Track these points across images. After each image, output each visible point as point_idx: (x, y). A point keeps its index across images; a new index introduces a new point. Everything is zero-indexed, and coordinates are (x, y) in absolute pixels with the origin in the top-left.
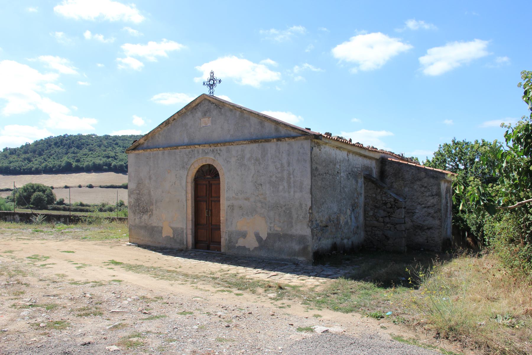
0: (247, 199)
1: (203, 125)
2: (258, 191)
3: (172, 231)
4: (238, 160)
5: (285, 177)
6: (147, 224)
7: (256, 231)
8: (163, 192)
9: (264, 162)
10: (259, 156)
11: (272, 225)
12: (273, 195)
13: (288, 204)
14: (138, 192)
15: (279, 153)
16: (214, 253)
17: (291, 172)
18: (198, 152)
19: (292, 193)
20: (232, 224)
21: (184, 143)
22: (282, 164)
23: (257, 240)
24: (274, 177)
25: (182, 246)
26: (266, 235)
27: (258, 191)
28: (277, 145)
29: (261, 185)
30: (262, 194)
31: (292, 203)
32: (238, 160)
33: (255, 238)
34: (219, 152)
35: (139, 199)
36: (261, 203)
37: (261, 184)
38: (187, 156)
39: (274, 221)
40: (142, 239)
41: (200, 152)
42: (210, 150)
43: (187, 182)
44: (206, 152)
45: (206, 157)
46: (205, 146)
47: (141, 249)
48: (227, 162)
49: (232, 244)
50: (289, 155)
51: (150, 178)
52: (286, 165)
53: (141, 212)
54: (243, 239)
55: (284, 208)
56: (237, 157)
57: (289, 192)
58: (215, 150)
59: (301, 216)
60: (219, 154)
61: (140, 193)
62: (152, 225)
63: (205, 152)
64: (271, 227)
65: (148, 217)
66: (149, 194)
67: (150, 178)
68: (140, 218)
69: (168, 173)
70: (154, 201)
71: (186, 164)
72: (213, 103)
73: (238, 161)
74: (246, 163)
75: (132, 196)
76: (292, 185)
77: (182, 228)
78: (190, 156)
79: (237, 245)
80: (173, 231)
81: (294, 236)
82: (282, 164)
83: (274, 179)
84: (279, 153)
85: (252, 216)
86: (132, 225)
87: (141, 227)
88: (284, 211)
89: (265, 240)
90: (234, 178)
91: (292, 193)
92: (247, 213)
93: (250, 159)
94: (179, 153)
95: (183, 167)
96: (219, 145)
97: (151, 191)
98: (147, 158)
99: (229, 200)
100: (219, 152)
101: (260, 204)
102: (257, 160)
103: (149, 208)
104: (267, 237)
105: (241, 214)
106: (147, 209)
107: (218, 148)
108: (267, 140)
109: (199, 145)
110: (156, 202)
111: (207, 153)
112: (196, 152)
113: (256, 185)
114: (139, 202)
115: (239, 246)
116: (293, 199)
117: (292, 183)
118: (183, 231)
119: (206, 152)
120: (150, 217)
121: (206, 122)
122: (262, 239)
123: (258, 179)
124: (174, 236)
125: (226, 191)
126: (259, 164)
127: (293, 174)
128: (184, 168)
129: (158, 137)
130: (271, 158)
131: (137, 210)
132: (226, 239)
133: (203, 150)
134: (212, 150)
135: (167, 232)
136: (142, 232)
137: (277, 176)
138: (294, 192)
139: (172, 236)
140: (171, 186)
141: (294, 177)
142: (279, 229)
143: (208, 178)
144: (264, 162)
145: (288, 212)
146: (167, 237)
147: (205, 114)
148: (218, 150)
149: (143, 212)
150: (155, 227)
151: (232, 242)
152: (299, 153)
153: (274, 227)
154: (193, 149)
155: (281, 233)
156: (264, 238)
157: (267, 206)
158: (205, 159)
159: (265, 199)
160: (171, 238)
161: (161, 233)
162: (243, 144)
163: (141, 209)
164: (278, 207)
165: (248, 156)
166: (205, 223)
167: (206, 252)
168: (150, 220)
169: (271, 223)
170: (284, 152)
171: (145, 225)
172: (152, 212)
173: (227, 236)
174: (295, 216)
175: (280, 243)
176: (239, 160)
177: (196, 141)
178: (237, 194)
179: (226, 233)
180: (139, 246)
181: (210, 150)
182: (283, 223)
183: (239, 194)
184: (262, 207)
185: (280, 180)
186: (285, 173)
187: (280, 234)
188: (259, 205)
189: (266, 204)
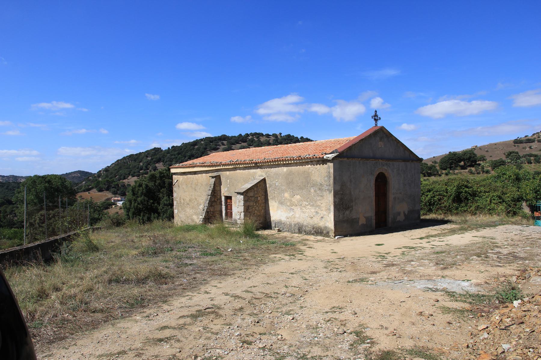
0: (401, 193)
1: (380, 146)
14: (342, 192)
51: (351, 181)
68: (344, 214)
77: (371, 216)
79: (397, 220)
108: (408, 161)
120: (351, 212)
121: (381, 144)
135: (362, 221)
139: (365, 223)
142: (411, 208)
147: (381, 139)
149: (346, 209)
150: (355, 218)
156: (406, 214)
161: (358, 222)
172: (352, 208)
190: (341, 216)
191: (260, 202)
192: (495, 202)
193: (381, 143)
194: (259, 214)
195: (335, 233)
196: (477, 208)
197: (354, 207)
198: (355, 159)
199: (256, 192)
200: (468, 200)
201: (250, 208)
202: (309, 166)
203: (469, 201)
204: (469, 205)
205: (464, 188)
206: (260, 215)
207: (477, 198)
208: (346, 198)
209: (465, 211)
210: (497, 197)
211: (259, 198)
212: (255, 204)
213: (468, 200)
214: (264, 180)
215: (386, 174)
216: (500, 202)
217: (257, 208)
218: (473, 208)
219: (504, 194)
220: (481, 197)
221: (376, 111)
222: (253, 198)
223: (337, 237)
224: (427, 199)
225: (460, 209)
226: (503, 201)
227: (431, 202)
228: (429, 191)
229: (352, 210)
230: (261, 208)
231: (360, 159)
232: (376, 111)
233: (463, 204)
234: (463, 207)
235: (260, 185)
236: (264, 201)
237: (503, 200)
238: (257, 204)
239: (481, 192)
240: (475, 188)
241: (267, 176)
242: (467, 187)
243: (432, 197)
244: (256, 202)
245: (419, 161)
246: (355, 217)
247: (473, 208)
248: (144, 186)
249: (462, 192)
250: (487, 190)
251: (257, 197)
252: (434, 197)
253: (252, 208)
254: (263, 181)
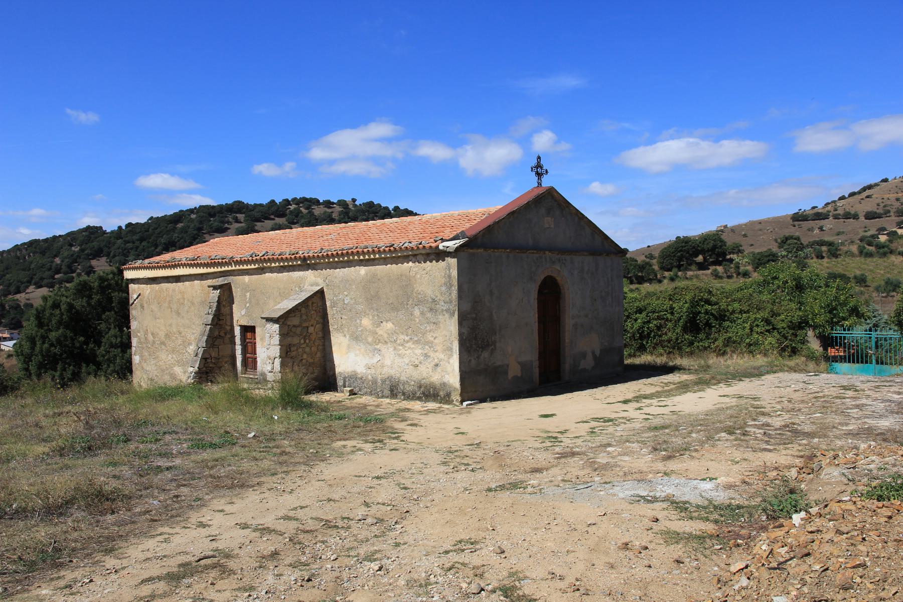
0: (586, 316)
1: (547, 226)
29: (595, 300)
60: (564, 264)
68: (478, 357)
72: (556, 201)
98: (487, 263)
106: (488, 341)
108: (600, 255)
111: (554, 262)
121: (548, 222)
135: (514, 371)
139: (519, 375)
142: (606, 344)
147: (549, 212)
156: (598, 356)
161: (506, 373)
163: (480, 342)
190: (473, 361)
191: (313, 337)
192: (759, 330)
193: (550, 218)
194: (311, 361)
195: (461, 395)
196: (728, 342)
197: (498, 345)
198: (500, 250)
199: (304, 317)
200: (710, 327)
201: (292, 349)
202: (411, 263)
203: (713, 329)
204: (712, 336)
205: (703, 305)
206: (313, 363)
207: (727, 323)
208: (482, 327)
209: (705, 348)
210: (762, 321)
211: (311, 329)
212: (302, 341)
213: (710, 327)
214: (320, 293)
215: (558, 279)
216: (768, 331)
217: (307, 349)
218: (719, 343)
219: (775, 314)
220: (735, 321)
221: (539, 158)
222: (299, 330)
223: (465, 404)
224: (636, 326)
225: (696, 344)
226: (774, 329)
227: (643, 332)
228: (640, 311)
230: (316, 349)
231: (508, 250)
232: (539, 158)
233: (702, 336)
234: (701, 340)
235: (313, 303)
236: (321, 334)
237: (773, 325)
238: (307, 341)
239: (733, 312)
240: (723, 305)
241: (328, 285)
242: (708, 302)
243: (644, 323)
244: (305, 336)
245: (620, 255)
246: (499, 363)
247: (719, 343)
248: (64, 307)
249: (700, 312)
250: (745, 308)
251: (308, 327)
252: (649, 322)
253: (297, 350)
254: (319, 295)
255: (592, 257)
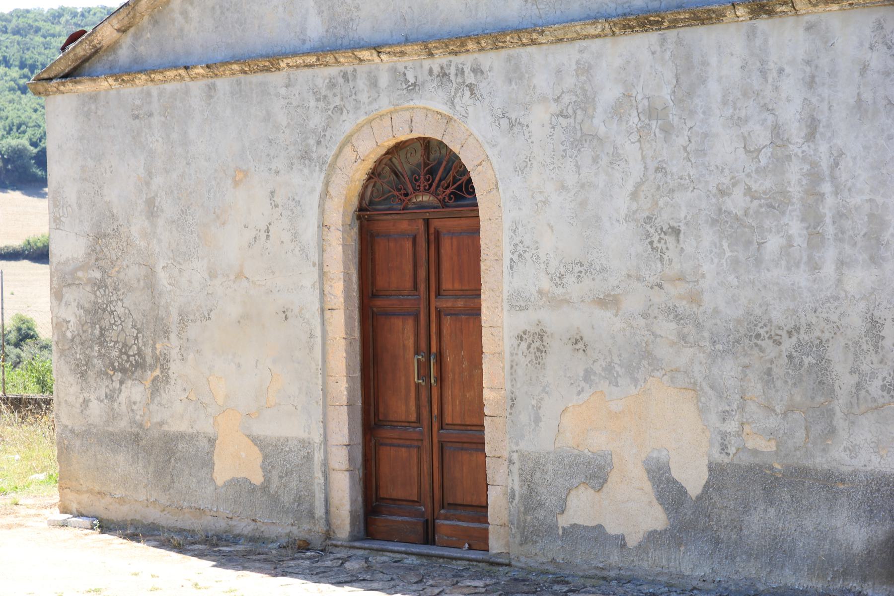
0: (609, 301)
2: (661, 259)
3: (256, 456)
4: (561, 114)
5: (795, 190)
6: (141, 426)
7: (655, 455)
8: (213, 275)
9: (690, 124)
10: (666, 93)
11: (732, 426)
12: (732, 279)
13: (809, 325)
14: (98, 275)
15: (763, 73)
16: (456, 559)
17: (825, 165)
18: (374, 83)
19: (829, 269)
20: (537, 420)
21: (304, 42)
22: (776, 130)
23: (661, 498)
24: (738, 194)
25: (306, 527)
26: (704, 476)
27: (661, 259)
28: (751, 35)
29: (676, 232)
30: (681, 278)
31: (827, 320)
32: (561, 114)
33: (648, 486)
34: (470, 78)
35: (104, 310)
36: (678, 318)
37: (671, 227)
38: (322, 105)
39: (742, 408)
40: (118, 493)
41: (384, 80)
42: (431, 72)
43: (323, 226)
44: (412, 81)
45: (411, 104)
46: (403, 54)
47: (113, 541)
48: (512, 126)
49: (541, 514)
50: (811, 83)
51: (152, 210)
52: (795, 132)
53: (114, 369)
54: (591, 491)
55: (788, 344)
56: (557, 100)
57: (815, 267)
58: (453, 71)
59: (878, 383)
60: (471, 87)
61: (109, 281)
62: (165, 428)
63: (407, 81)
64: (724, 435)
65: (148, 392)
66: (150, 284)
67: (152, 210)
68: (111, 397)
69: (236, 183)
70: (174, 317)
71: (319, 143)
73: (564, 122)
74: (602, 130)
75: (70, 295)
76: (830, 230)
77: (305, 444)
78: (337, 101)
79: (563, 521)
80: (266, 457)
81: (843, 481)
82: (776, 130)
83: (737, 202)
84: (763, 73)
85: (635, 381)
86: (72, 431)
87: (114, 441)
88: (790, 357)
89: (699, 498)
90: (545, 202)
91: (829, 269)
92: (609, 368)
93: (617, 111)
94: (283, 91)
95: (303, 158)
96: (471, 46)
97: (159, 269)
98: (136, 117)
99: (522, 309)
100: (470, 78)
101: (673, 325)
102: (652, 112)
103: (148, 351)
104: (707, 486)
105: (582, 374)
106: (140, 353)
107: (466, 60)
109: (377, 48)
110: (183, 320)
111: (414, 87)
112: (361, 83)
113: (648, 235)
114: (105, 323)
115: (574, 526)
116: (837, 298)
117: (828, 220)
118: (309, 458)
119: (412, 81)
120: (155, 389)
122: (682, 491)
123: (661, 203)
124: (268, 480)
125: (506, 262)
126: (667, 130)
127: (833, 178)
128: (310, 160)
129: (184, 13)
130: (725, 103)
131: (95, 361)
132: (513, 491)
133: (394, 70)
134: (436, 70)
136: (121, 461)
137: (754, 187)
138: (842, 263)
139: (258, 479)
140: (250, 246)
141: (837, 192)
143: (422, 206)
144: (689, 124)
145: (807, 360)
146: (235, 483)
148: (467, 71)
149: (123, 370)
150: (181, 436)
151: (541, 505)
152: (864, 69)
153: (738, 435)
154: (350, 69)
155: (777, 466)
157: (706, 334)
158: (407, 115)
159: (695, 298)
160: (253, 489)
161: (208, 464)
162: (586, 37)
163: (115, 353)
164: (758, 336)
165: (609, 93)
166: (413, 418)
167: (420, 555)
168: (153, 407)
169: (725, 416)
170: (788, 70)
171: (135, 430)
172: (165, 370)
173: (516, 478)
174: (845, 381)
175: (772, 511)
176: (566, 117)
177: (363, 30)
178: (559, 279)
179: (511, 462)
180: (105, 527)
181: (431, 72)
182: (785, 414)
183: (570, 279)
184: (683, 337)
185: (771, 206)
186: (795, 173)
187: (771, 468)
188: (667, 328)
189: (698, 326)
190: (94, 405)
197: (175, 368)
208: (120, 310)
229: (167, 378)
255: (651, 38)
